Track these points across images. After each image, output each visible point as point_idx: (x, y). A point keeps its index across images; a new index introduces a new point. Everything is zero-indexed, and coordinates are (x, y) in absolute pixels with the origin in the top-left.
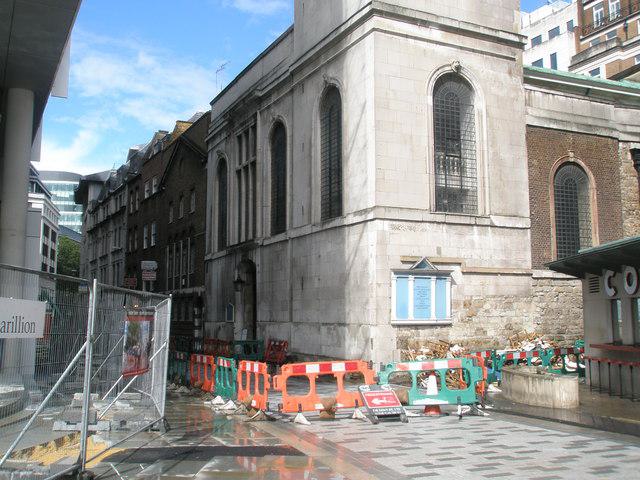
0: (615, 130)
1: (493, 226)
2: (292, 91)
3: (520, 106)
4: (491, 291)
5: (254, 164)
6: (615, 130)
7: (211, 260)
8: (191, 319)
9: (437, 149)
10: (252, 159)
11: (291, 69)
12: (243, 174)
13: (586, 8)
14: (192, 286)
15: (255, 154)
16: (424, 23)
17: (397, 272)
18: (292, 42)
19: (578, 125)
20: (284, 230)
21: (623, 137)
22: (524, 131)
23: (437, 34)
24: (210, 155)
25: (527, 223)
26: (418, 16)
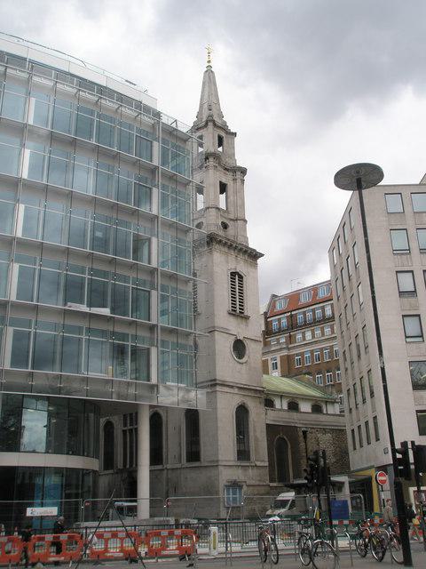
3: (263, 416)
13: (269, 320)
16: (232, 387)
19: (284, 422)
20: (162, 463)
23: (236, 391)
25: (267, 464)
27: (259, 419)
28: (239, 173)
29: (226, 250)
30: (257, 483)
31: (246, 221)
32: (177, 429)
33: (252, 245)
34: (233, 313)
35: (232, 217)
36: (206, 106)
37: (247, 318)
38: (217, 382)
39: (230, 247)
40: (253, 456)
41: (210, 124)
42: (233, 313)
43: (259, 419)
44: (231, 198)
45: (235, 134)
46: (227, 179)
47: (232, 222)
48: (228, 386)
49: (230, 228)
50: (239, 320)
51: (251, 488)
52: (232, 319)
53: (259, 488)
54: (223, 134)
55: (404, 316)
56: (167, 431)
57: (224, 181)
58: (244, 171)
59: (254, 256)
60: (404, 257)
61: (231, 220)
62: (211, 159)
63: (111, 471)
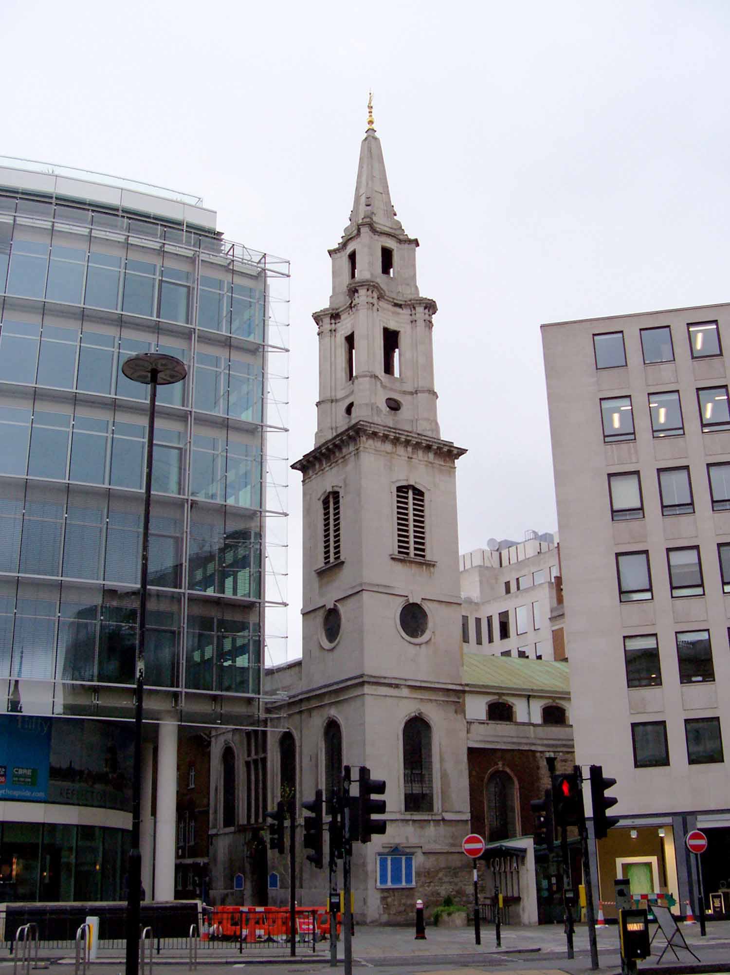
0: (534, 744)
1: (443, 820)
2: (301, 712)
4: (443, 866)
5: (264, 760)
6: (534, 744)
7: (216, 835)
8: (191, 888)
9: (405, 768)
10: (263, 756)
11: (300, 697)
12: (252, 767)
14: (191, 856)
15: (265, 750)
16: (397, 686)
17: (380, 854)
18: (300, 672)
21: (540, 749)
22: (465, 751)
23: (405, 692)
24: (213, 739)
25: (467, 816)
26: (393, 682)
27: (452, 744)
28: (420, 309)
29: (388, 447)
30: (446, 849)
31: (435, 395)
32: (314, 760)
33: (445, 436)
34: (402, 556)
35: (410, 389)
36: (363, 199)
37: (430, 565)
38: (365, 679)
39: (396, 441)
40: (437, 805)
41: (365, 230)
42: (402, 556)
43: (452, 744)
44: (408, 355)
45: (416, 243)
46: (396, 321)
47: (409, 397)
48: (390, 685)
49: (404, 409)
50: (414, 569)
51: (432, 858)
52: (399, 566)
53: (450, 857)
54: (390, 244)
55: (618, 555)
56: (301, 762)
57: (392, 326)
58: (431, 306)
59: (450, 454)
60: (624, 446)
61: (405, 393)
62: (362, 292)
63: (232, 829)
